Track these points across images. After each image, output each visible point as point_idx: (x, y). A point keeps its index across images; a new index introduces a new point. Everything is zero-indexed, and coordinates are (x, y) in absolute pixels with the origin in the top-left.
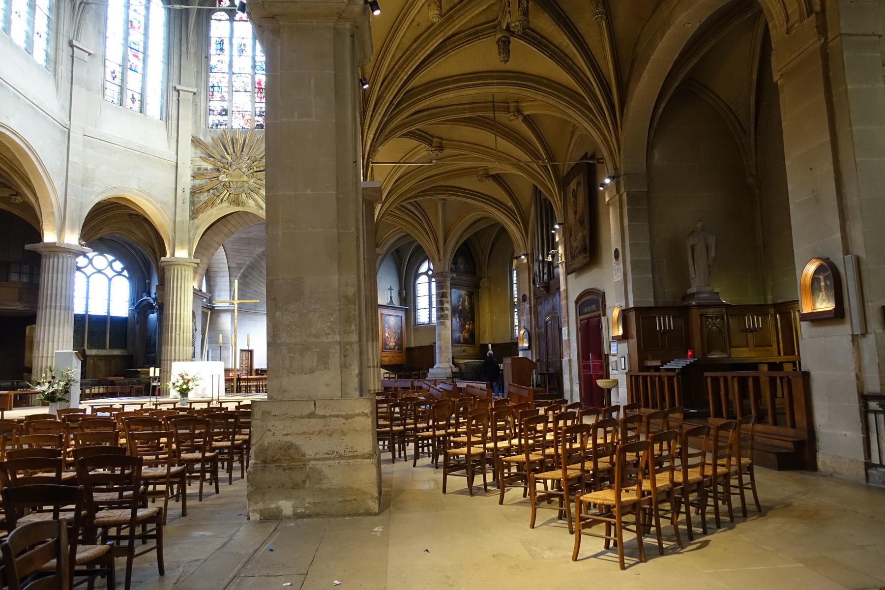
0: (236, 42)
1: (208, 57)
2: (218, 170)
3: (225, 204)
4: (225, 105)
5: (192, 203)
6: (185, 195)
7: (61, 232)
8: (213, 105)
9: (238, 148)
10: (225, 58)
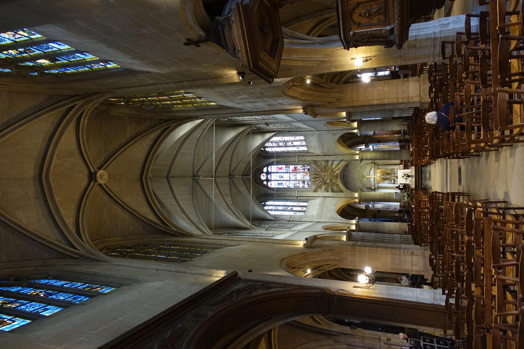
0: (278, 179)
1: (285, 188)
2: (325, 183)
3: (338, 181)
4: (301, 182)
5: (337, 192)
6: (335, 194)
7: (352, 224)
8: (301, 186)
9: (318, 176)
10: (284, 182)
